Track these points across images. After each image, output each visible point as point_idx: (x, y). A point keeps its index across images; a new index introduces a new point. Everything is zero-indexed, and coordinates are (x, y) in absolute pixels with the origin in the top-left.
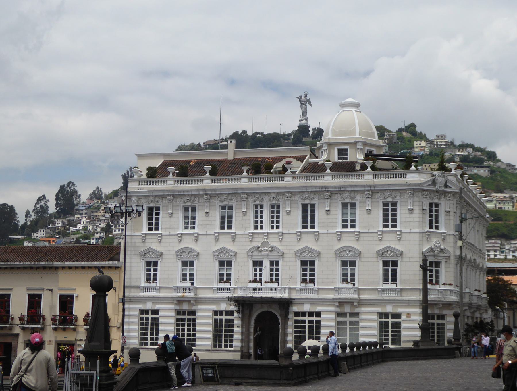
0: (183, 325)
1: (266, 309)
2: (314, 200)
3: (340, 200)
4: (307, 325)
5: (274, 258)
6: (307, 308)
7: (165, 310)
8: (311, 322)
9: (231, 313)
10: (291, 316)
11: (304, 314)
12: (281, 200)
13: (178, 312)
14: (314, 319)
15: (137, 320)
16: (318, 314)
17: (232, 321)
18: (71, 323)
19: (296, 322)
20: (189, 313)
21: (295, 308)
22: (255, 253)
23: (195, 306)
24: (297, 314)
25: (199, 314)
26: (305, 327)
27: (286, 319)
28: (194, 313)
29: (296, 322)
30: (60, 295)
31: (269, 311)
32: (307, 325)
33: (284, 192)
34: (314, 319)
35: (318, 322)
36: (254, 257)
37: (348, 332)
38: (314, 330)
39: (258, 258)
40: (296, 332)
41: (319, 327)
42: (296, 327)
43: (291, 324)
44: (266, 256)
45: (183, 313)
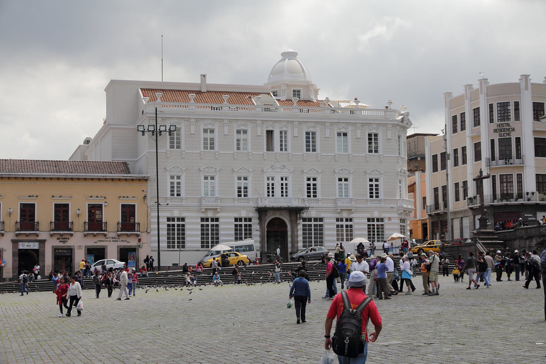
0: (174, 230)
1: (278, 216)
2: (316, 128)
3: (235, 127)
4: (313, 228)
5: (284, 175)
6: (313, 214)
7: (191, 218)
8: (315, 225)
9: (250, 220)
10: (301, 222)
11: (310, 220)
12: (289, 128)
13: (202, 219)
14: (318, 223)
15: (166, 227)
16: (321, 220)
17: (250, 226)
18: (133, 229)
19: (304, 225)
20: (212, 220)
21: (305, 215)
22: (270, 170)
23: (219, 214)
24: (304, 220)
25: (221, 220)
26: (311, 230)
27: (294, 223)
28: (217, 220)
29: (304, 225)
30: (55, 204)
31: (280, 219)
32: (313, 228)
33: (356, 123)
34: (318, 223)
35: (321, 226)
36: (268, 173)
37: (345, 233)
38: (307, 232)
39: (271, 175)
40: (304, 234)
41: (322, 230)
42: (304, 230)
43: (300, 227)
44: (279, 173)
45: (207, 220)
